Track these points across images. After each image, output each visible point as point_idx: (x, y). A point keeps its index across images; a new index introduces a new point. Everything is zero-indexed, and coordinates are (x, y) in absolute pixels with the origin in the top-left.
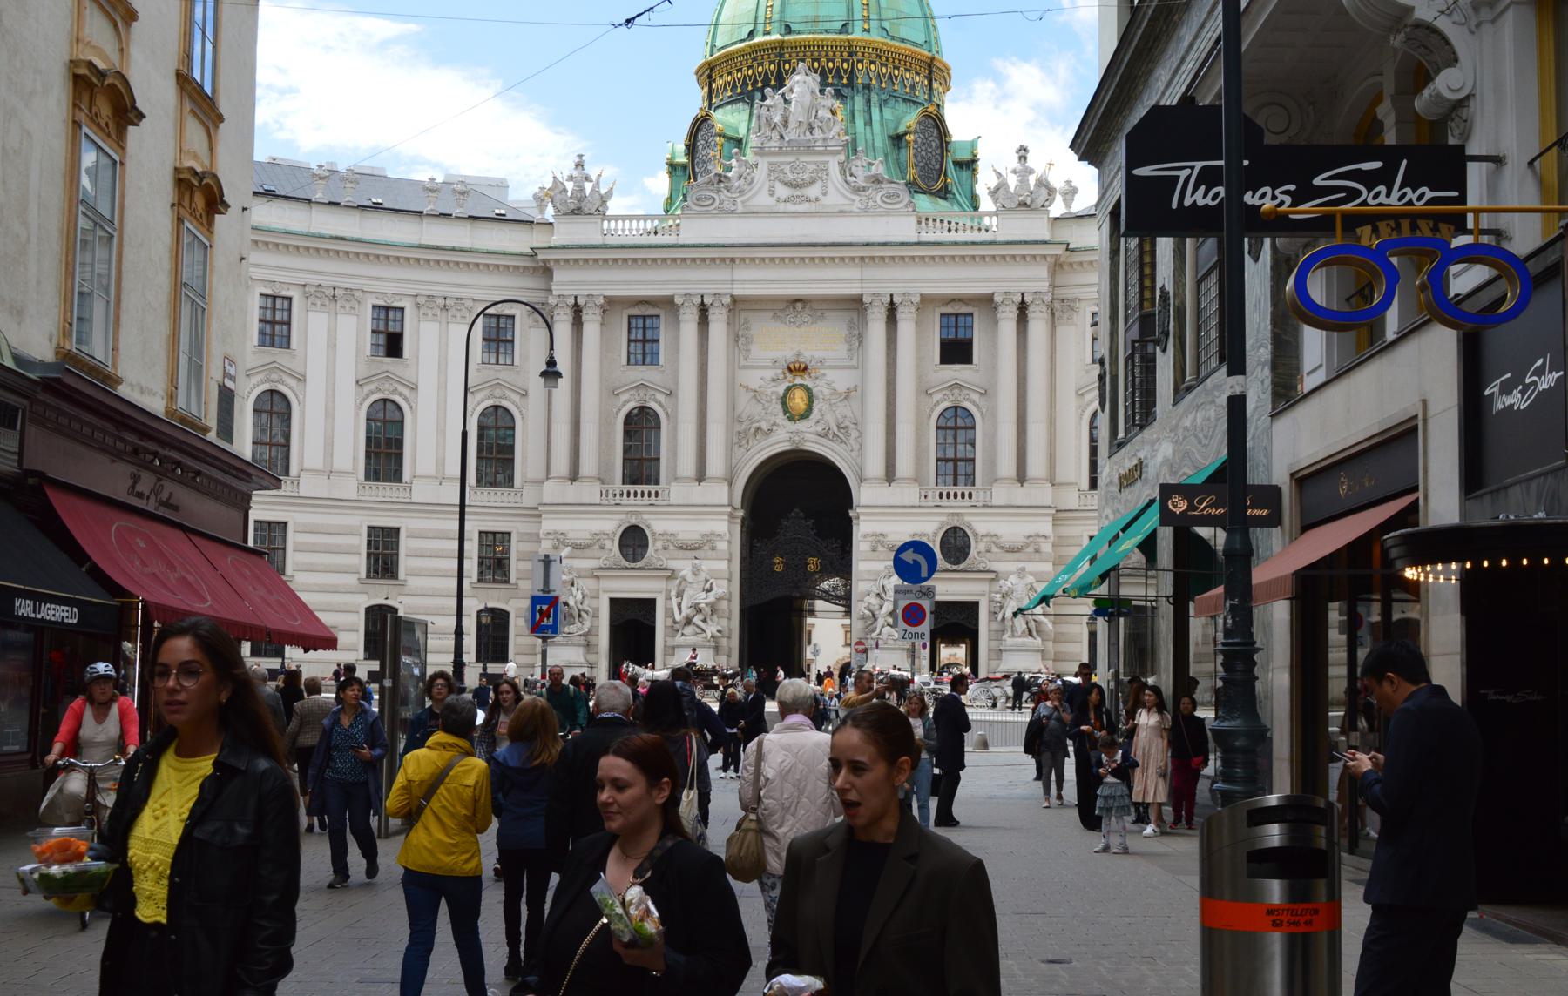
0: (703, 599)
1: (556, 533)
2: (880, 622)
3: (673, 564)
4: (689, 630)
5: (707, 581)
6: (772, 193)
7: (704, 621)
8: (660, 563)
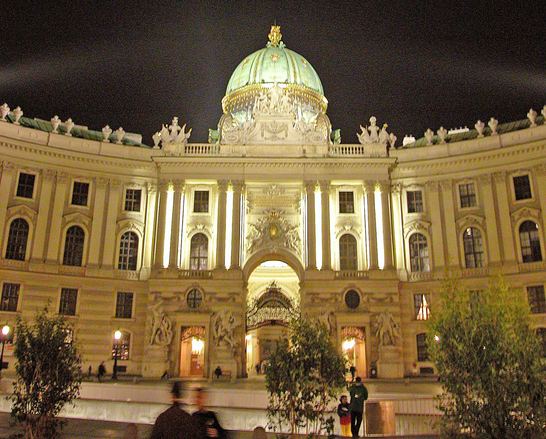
0: (229, 328)
1: (156, 292)
3: (214, 309)
5: (231, 318)
6: (262, 135)
7: (230, 338)
8: (206, 308)
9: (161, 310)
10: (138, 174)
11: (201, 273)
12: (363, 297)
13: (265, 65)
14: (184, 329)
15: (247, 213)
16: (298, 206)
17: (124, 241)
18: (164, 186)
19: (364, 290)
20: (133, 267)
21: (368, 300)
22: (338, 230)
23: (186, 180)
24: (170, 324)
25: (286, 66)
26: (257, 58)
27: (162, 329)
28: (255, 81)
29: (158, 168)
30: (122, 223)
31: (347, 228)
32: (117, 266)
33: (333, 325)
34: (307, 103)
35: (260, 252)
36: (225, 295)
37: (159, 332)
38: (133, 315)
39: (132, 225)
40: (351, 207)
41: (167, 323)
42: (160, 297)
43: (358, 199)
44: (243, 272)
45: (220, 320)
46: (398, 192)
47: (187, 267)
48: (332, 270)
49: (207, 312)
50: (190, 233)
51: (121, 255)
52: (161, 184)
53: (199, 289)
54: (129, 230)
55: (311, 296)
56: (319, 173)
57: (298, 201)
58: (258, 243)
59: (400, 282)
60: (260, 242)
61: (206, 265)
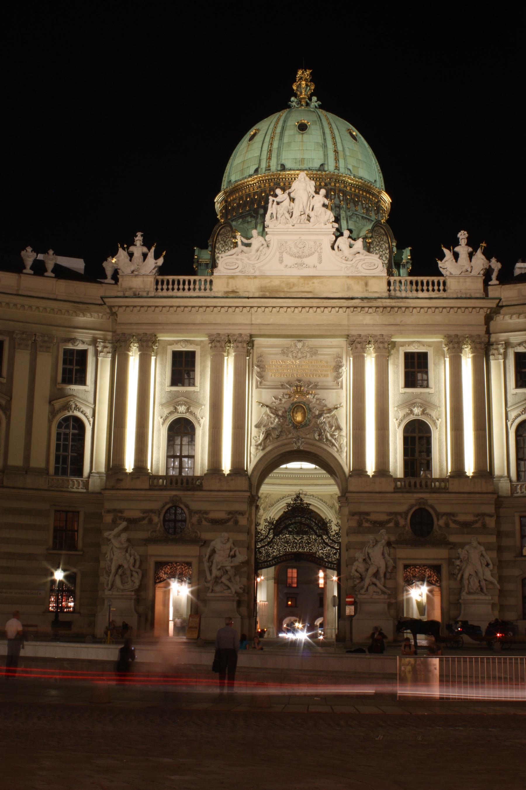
0: (228, 565)
1: (115, 511)
2: (367, 581)
3: (206, 536)
4: (218, 588)
5: (231, 551)
6: (281, 261)
7: (229, 580)
9: (124, 536)
10: (81, 325)
11: (185, 480)
12: (438, 519)
13: (286, 140)
14: (159, 565)
15: (257, 387)
16: (338, 376)
17: (63, 430)
18: (123, 344)
19: (441, 509)
20: (79, 471)
21: (447, 525)
22: (401, 414)
23: (158, 335)
24: (138, 557)
25: (320, 140)
26: (272, 126)
27: (126, 566)
28: (269, 166)
29: (114, 314)
30: (58, 404)
31: (416, 410)
32: (52, 470)
33: (391, 563)
34: (356, 204)
35: (276, 448)
36: (222, 515)
37: (120, 571)
38: (80, 545)
39: (74, 406)
40: (425, 377)
41: (132, 558)
42: (121, 518)
43: (435, 364)
44: (249, 478)
45: (214, 552)
46: (499, 354)
47: (162, 472)
48: (391, 476)
49: (196, 541)
50: (167, 417)
51: (58, 453)
52: (118, 341)
53: (182, 506)
54: (71, 413)
55: (357, 517)
56: (371, 322)
57: (338, 367)
58: (274, 435)
59: (499, 497)
60: (277, 433)
61: (193, 468)
